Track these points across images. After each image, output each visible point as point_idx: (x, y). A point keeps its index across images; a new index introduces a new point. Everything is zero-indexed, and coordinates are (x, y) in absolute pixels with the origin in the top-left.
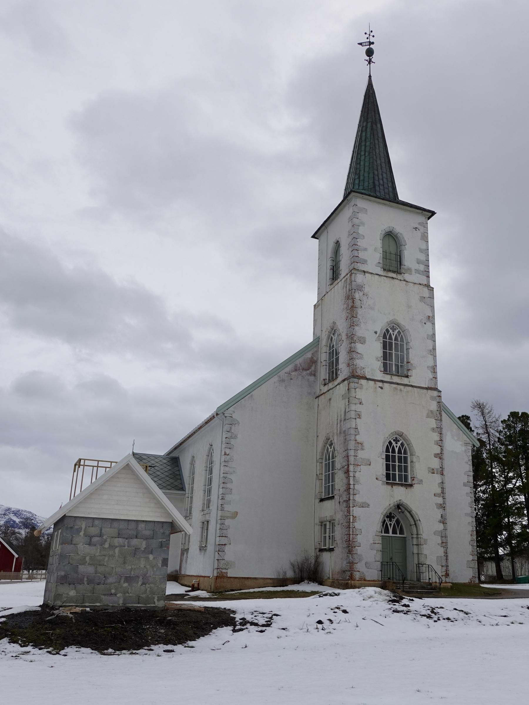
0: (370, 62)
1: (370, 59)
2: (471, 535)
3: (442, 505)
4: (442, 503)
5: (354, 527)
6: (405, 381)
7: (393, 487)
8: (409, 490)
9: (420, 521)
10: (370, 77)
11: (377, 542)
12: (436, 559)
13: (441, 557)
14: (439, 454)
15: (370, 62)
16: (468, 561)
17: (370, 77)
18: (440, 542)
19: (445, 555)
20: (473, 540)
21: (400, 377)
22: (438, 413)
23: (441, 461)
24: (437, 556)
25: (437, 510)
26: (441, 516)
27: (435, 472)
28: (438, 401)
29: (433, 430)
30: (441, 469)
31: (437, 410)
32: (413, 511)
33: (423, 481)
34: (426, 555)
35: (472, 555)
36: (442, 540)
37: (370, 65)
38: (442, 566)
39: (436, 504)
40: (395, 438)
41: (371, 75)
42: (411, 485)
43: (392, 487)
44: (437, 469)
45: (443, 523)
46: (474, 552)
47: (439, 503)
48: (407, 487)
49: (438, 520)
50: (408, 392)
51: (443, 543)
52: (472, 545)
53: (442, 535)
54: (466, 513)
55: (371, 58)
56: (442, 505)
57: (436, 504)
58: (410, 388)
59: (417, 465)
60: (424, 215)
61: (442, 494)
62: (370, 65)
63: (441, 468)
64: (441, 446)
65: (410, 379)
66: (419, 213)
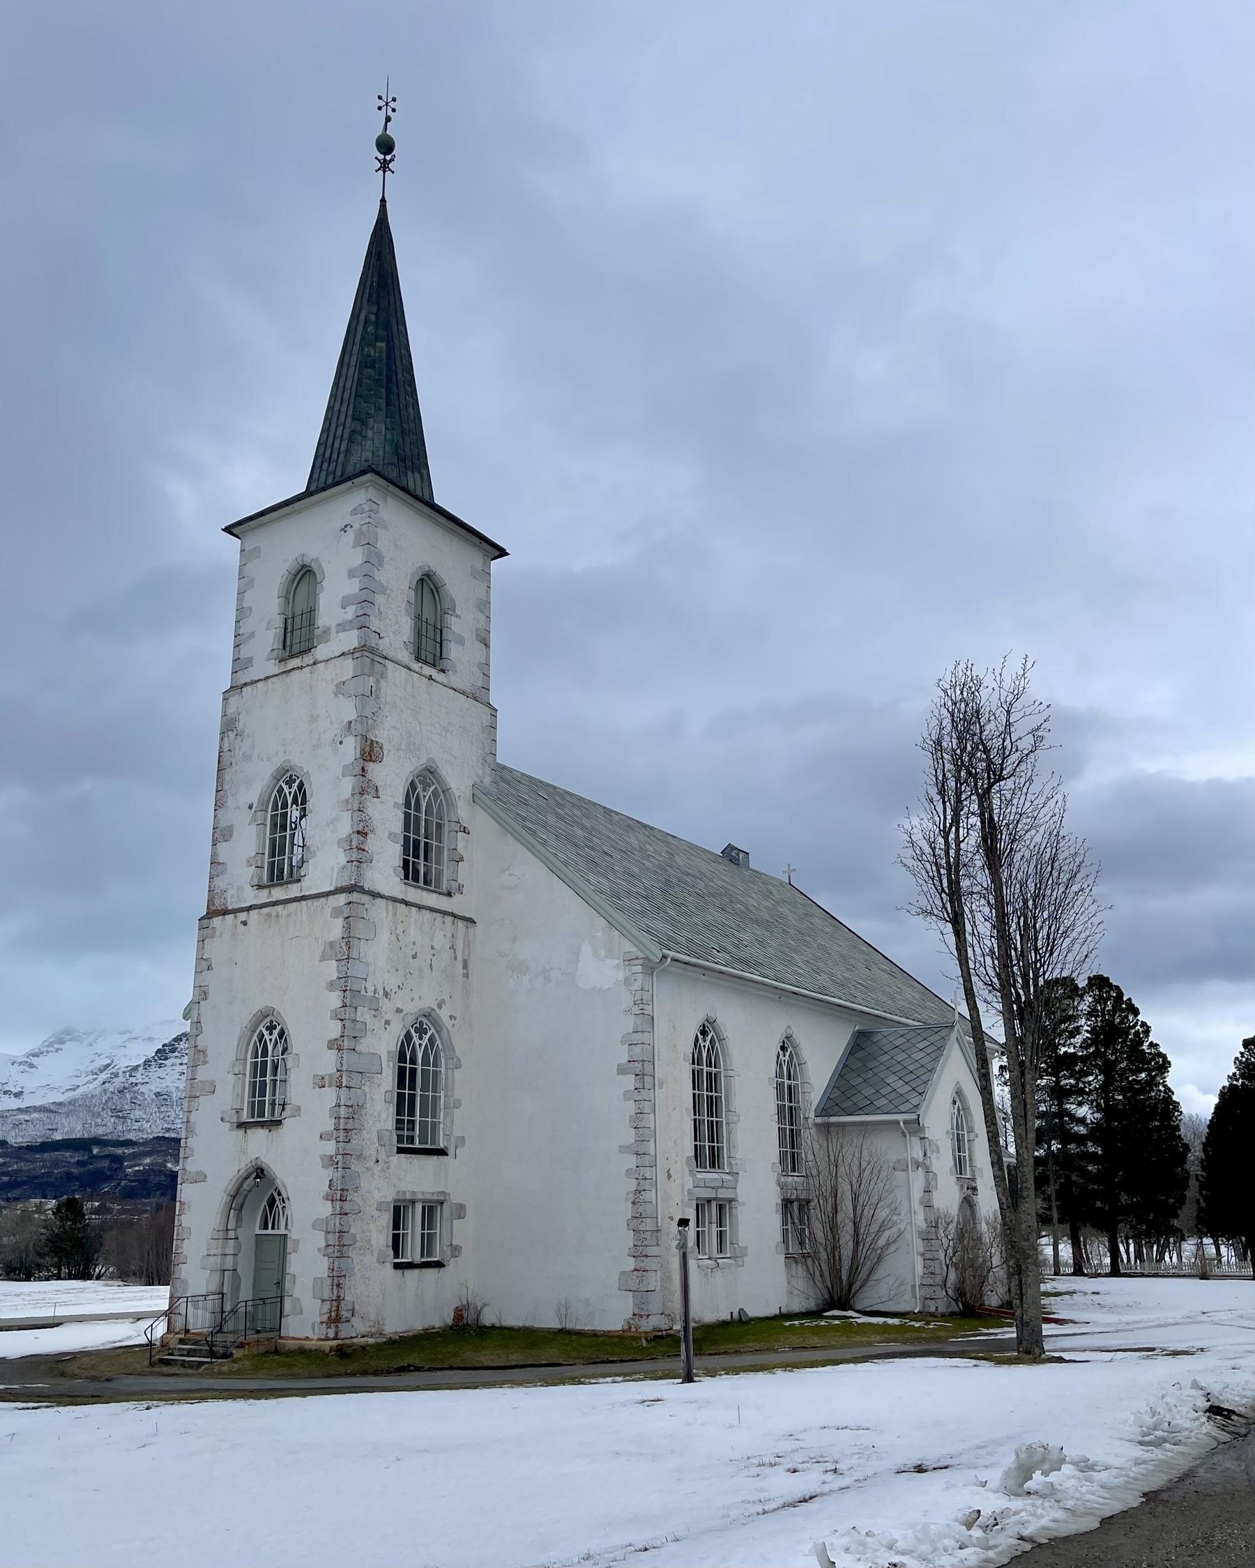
0: (384, 166)
1: (385, 159)
2: (633, 1203)
3: (334, 1158)
4: (334, 1153)
5: (181, 1225)
6: (294, 891)
7: (248, 1131)
8: (277, 1132)
9: (289, 1199)
10: (383, 201)
11: (212, 1253)
12: (311, 1285)
13: (322, 1278)
14: (337, 1039)
15: (384, 166)
16: (623, 1273)
17: (383, 201)
18: (324, 1244)
19: (331, 1275)
20: (638, 1215)
21: (285, 886)
22: (343, 944)
23: (339, 1054)
24: (315, 1279)
25: (322, 1169)
26: (330, 1185)
27: (327, 1085)
28: (346, 915)
29: (331, 986)
30: (339, 1073)
31: (343, 938)
32: (278, 1180)
33: (302, 1109)
34: (295, 1276)
35: (634, 1257)
36: (327, 1241)
37: (384, 173)
38: (323, 1301)
39: (322, 1157)
40: (268, 1024)
41: (386, 199)
42: (279, 1123)
43: (246, 1132)
44: (330, 1076)
45: (332, 1201)
46: (641, 1248)
47: (328, 1154)
48: (272, 1128)
49: (322, 1194)
50: (289, 915)
51: (328, 1246)
52: (634, 1230)
53: (327, 1228)
54: (621, 1144)
55: (388, 157)
56: (334, 1158)
57: (322, 1157)
58: (295, 904)
59: (293, 1076)
60: (361, 485)
61: (335, 1132)
62: (384, 173)
63: (338, 1071)
64: (342, 1020)
65: (303, 883)
66: (349, 489)
